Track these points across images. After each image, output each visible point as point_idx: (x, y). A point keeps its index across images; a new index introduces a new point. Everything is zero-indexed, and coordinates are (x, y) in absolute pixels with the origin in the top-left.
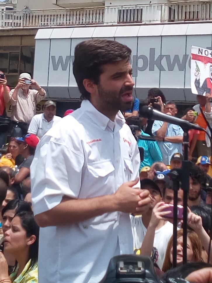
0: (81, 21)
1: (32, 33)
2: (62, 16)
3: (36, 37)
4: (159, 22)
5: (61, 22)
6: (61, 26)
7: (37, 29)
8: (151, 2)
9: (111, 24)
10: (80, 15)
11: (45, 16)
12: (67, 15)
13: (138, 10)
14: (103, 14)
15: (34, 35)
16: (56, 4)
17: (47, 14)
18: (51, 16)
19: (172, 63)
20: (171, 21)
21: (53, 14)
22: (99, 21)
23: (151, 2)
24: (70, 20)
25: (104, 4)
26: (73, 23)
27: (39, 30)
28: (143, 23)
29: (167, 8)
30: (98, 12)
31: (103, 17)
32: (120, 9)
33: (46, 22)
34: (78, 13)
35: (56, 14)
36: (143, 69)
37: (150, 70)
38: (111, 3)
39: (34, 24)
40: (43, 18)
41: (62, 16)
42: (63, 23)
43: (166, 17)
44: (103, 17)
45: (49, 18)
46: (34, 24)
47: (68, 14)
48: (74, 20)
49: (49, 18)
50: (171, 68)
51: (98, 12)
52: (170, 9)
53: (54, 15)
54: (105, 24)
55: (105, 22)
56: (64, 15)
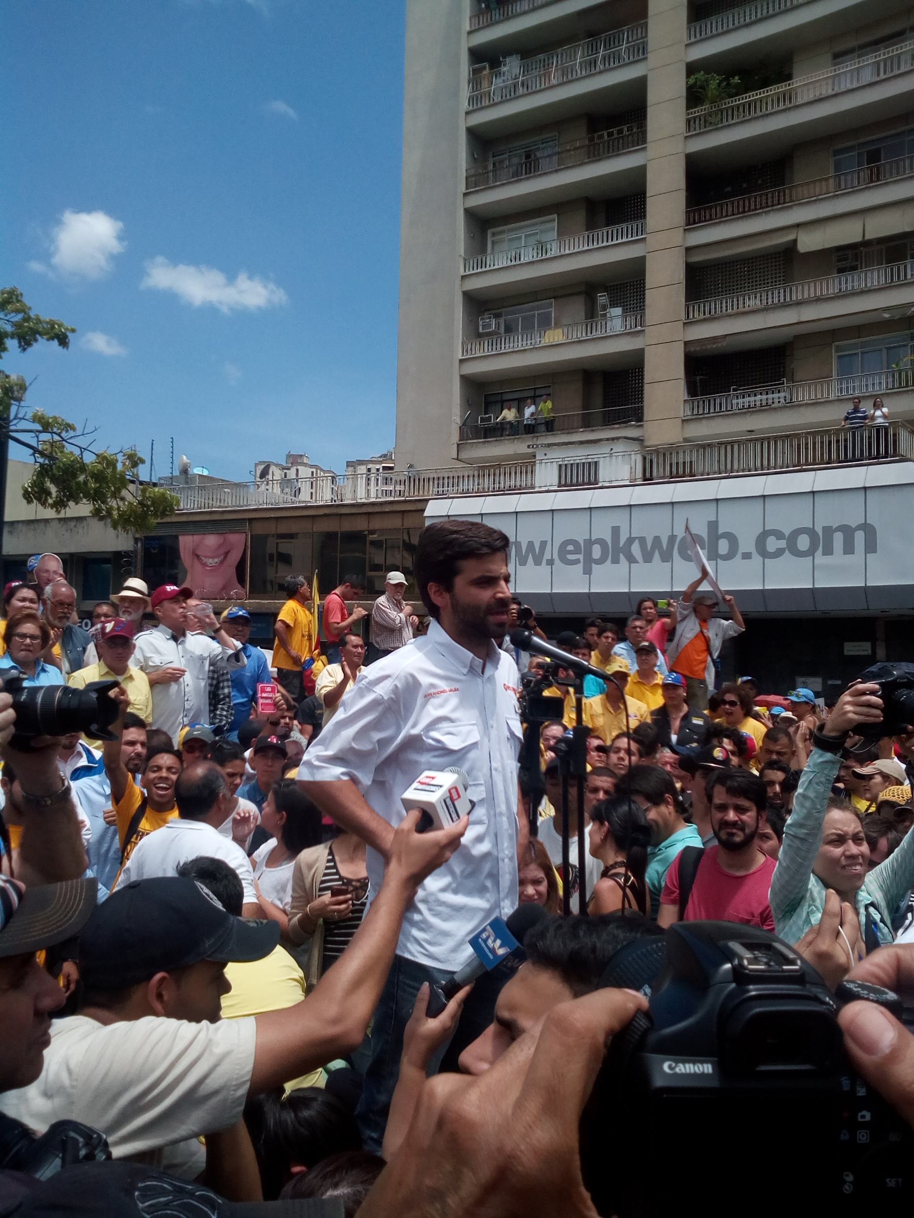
0: (497, 486)
1: (419, 506)
2: (466, 479)
3: (426, 514)
4: (627, 483)
5: (466, 488)
6: (466, 494)
7: (427, 500)
8: (612, 449)
9: (546, 489)
10: (494, 475)
11: (438, 478)
12: (474, 476)
13: (590, 463)
14: (532, 472)
15: (423, 510)
16: (457, 459)
17: (441, 475)
18: (448, 478)
19: (649, 548)
20: (648, 479)
21: (451, 475)
22: (526, 485)
23: (612, 449)
24: (478, 485)
25: (535, 456)
26: (484, 489)
27: (430, 501)
28: (600, 485)
29: (639, 459)
30: (524, 470)
31: (532, 477)
32: (560, 463)
33: (441, 489)
34: (492, 471)
35: (456, 475)
36: (601, 561)
37: (613, 562)
38: (545, 454)
39: (416, 493)
40: (436, 482)
41: (466, 479)
42: (468, 490)
43: (639, 474)
44: (532, 477)
45: (446, 481)
46: (416, 493)
47: (476, 473)
48: (487, 483)
49: (446, 481)
50: (648, 558)
51: (524, 470)
52: (644, 459)
53: (453, 477)
54: (537, 490)
55: (537, 485)
56: (468, 476)
